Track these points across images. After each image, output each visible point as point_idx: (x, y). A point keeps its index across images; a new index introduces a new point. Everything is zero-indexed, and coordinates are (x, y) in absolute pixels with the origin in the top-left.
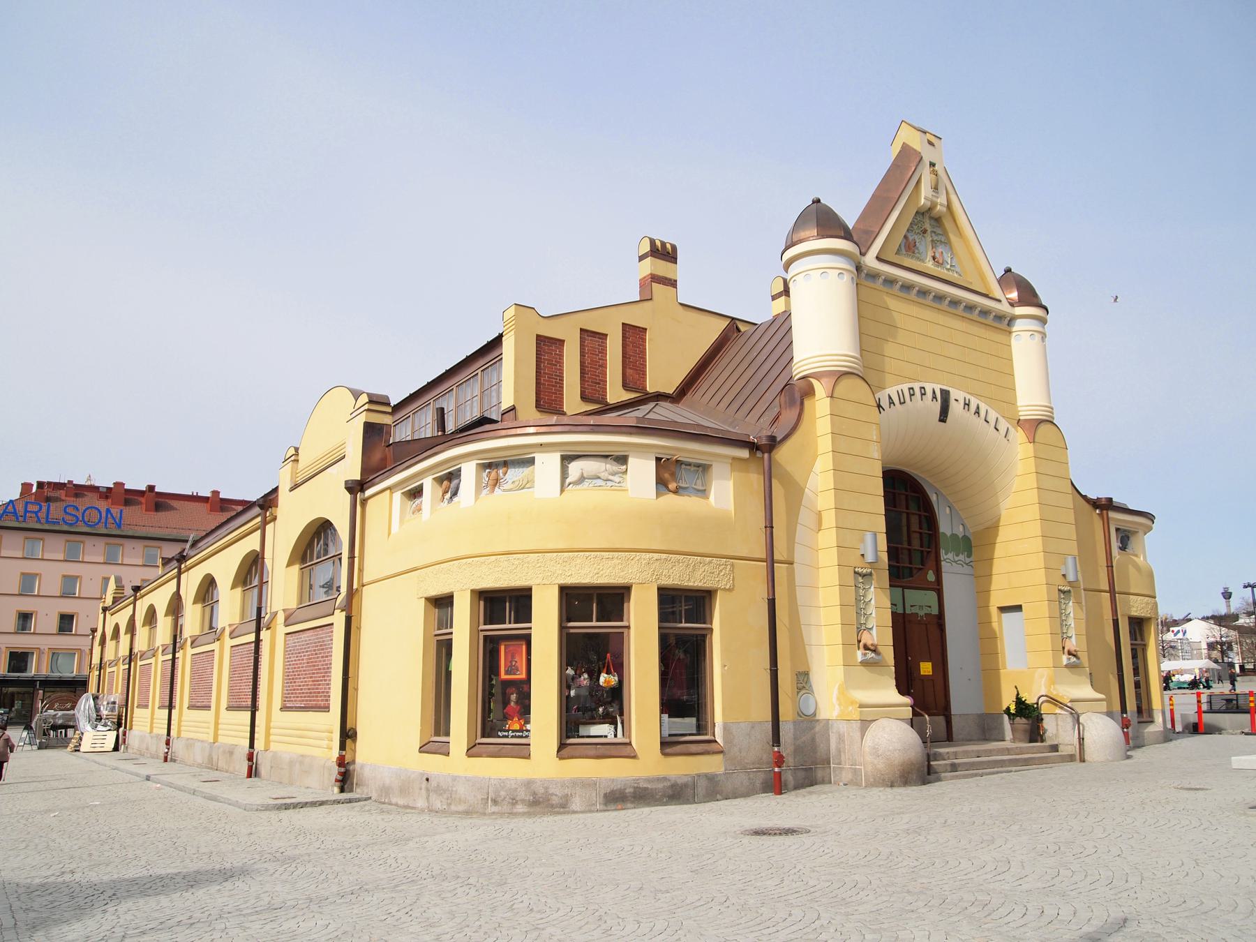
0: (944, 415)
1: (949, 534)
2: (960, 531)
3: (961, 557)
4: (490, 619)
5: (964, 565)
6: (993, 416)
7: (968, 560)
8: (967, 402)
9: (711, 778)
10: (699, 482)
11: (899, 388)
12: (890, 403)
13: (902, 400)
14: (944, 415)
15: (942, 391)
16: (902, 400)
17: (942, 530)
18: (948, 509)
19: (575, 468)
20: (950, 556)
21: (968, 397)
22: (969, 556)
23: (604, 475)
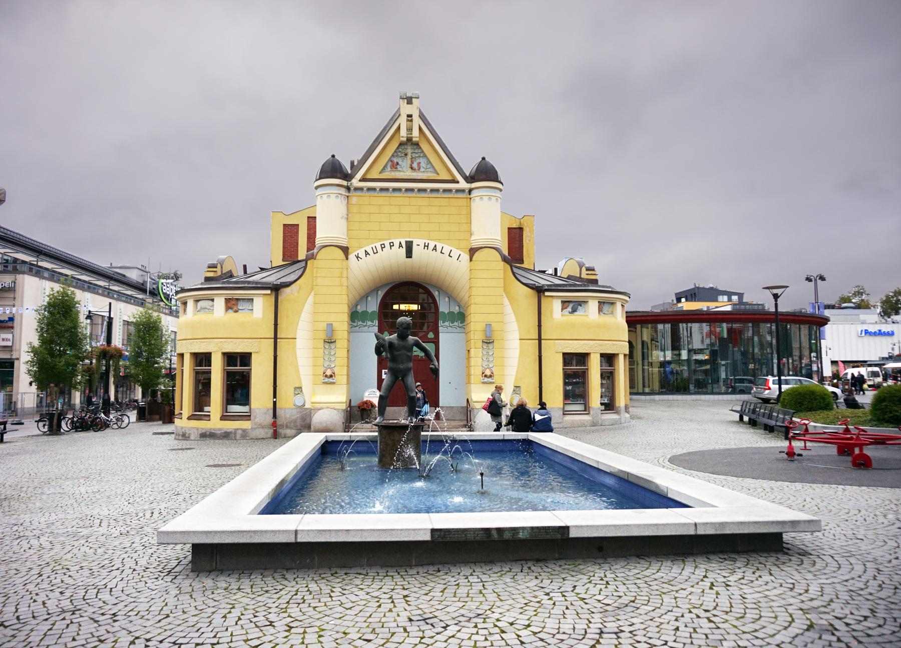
0: (409, 254)
1: (446, 312)
2: (456, 309)
3: (456, 324)
4: (229, 365)
5: (458, 328)
6: (446, 250)
7: (460, 325)
8: (426, 245)
9: (244, 431)
10: (250, 306)
11: (376, 244)
12: (366, 255)
13: (375, 251)
14: (409, 254)
15: (406, 242)
16: (375, 251)
17: (441, 310)
18: (447, 299)
19: (200, 304)
20: (447, 324)
21: (425, 241)
22: (461, 323)
23: (208, 307)
